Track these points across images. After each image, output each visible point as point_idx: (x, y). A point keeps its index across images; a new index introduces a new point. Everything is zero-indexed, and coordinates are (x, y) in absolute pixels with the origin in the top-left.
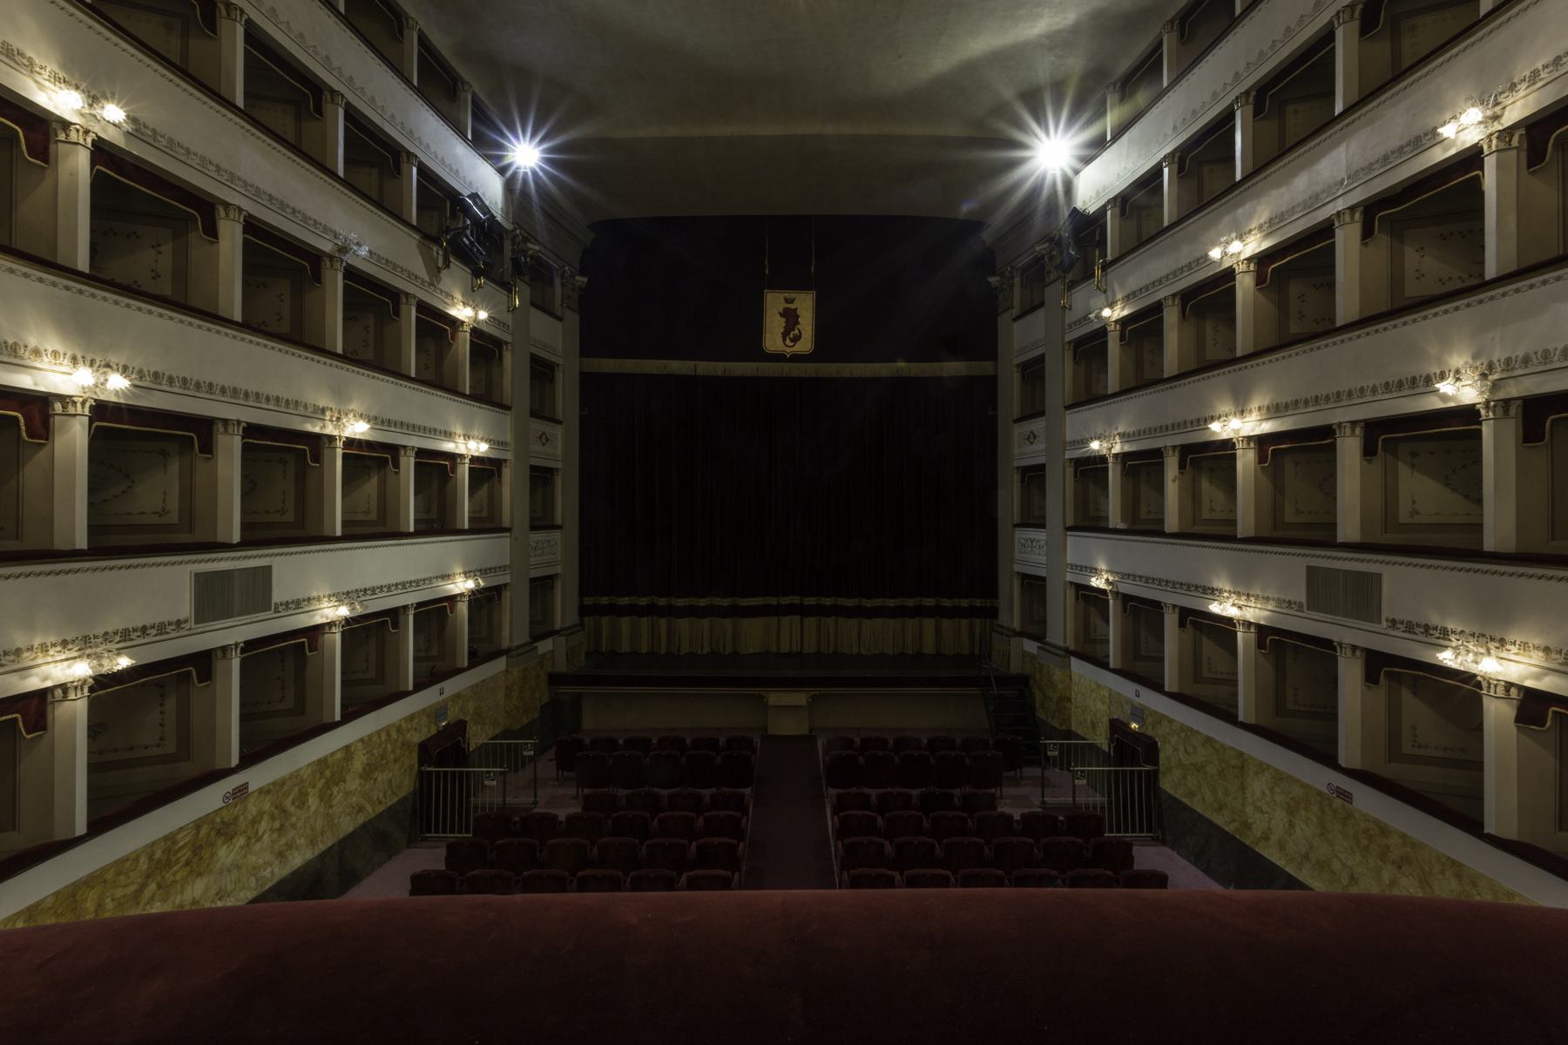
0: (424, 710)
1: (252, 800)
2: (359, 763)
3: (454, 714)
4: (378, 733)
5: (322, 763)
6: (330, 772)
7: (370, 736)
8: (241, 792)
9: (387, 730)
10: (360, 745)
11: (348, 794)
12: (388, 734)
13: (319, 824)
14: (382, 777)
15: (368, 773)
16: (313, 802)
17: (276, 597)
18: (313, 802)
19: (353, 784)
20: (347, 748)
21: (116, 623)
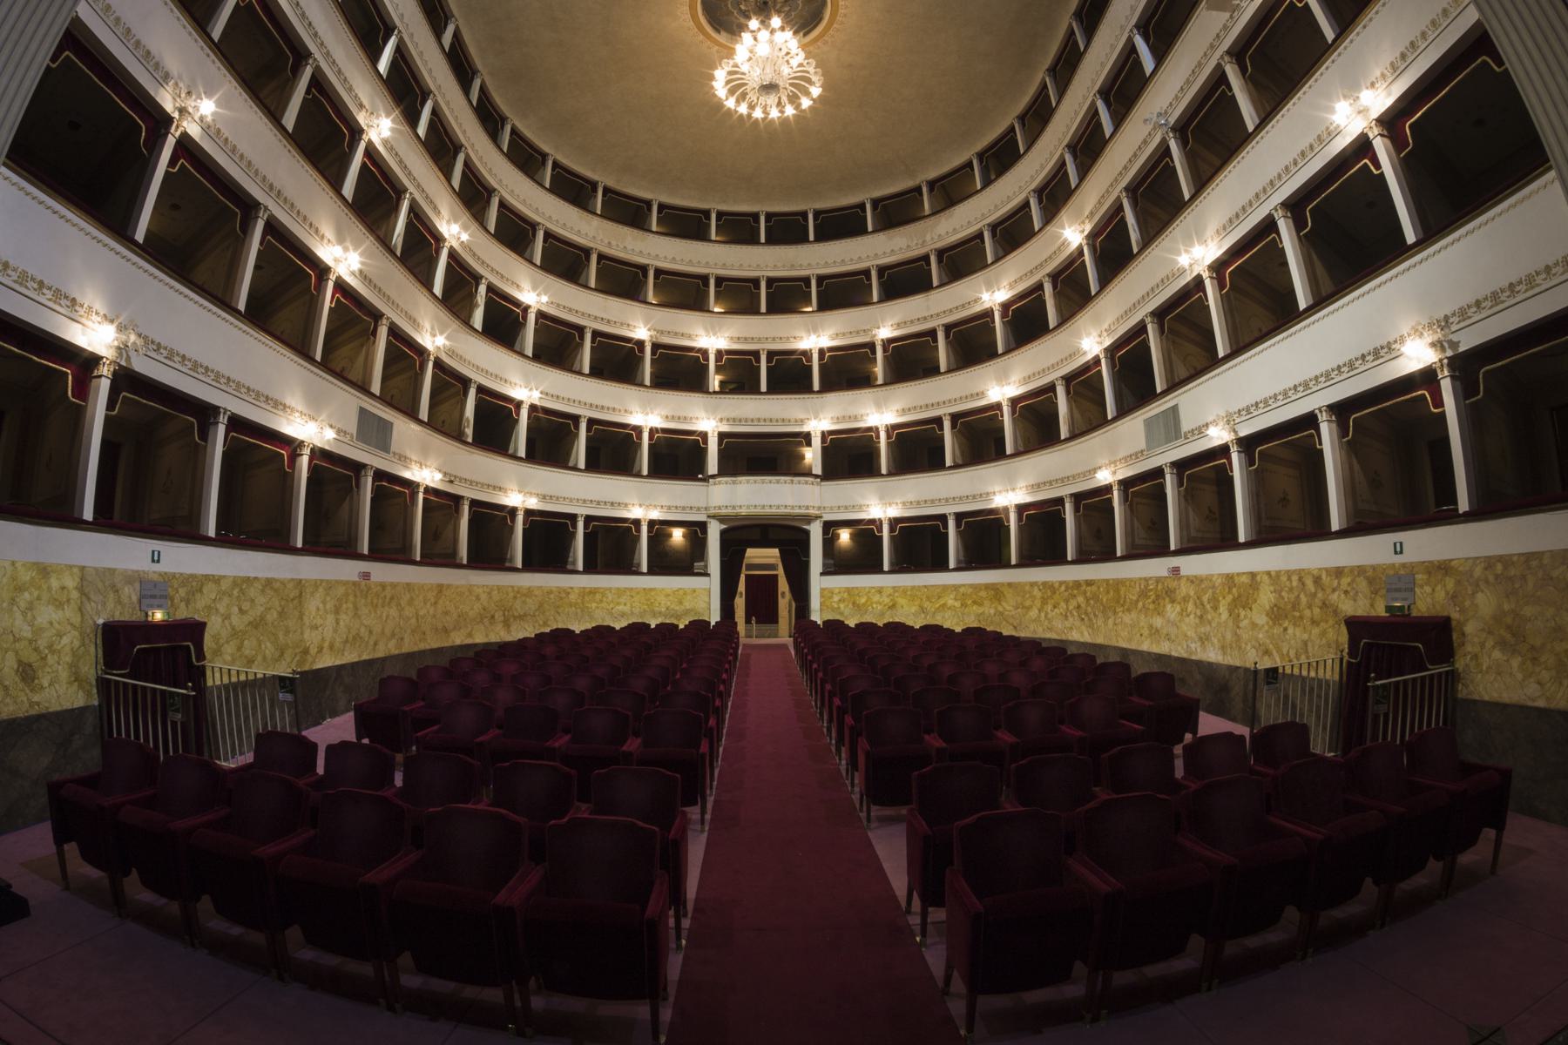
0: (1361, 570)
1: (1183, 582)
2: (1266, 597)
3: (1427, 601)
4: (1289, 574)
5: (1230, 579)
6: (1242, 591)
7: (1278, 573)
8: (1176, 570)
9: (1301, 574)
10: (1266, 578)
11: (1254, 625)
12: (1300, 579)
13: (1229, 636)
14: (1296, 634)
15: (1277, 614)
16: (1223, 609)
17: (1186, 426)
18: (1223, 609)
19: (1262, 620)
20: (1253, 575)
21: (1122, 454)
